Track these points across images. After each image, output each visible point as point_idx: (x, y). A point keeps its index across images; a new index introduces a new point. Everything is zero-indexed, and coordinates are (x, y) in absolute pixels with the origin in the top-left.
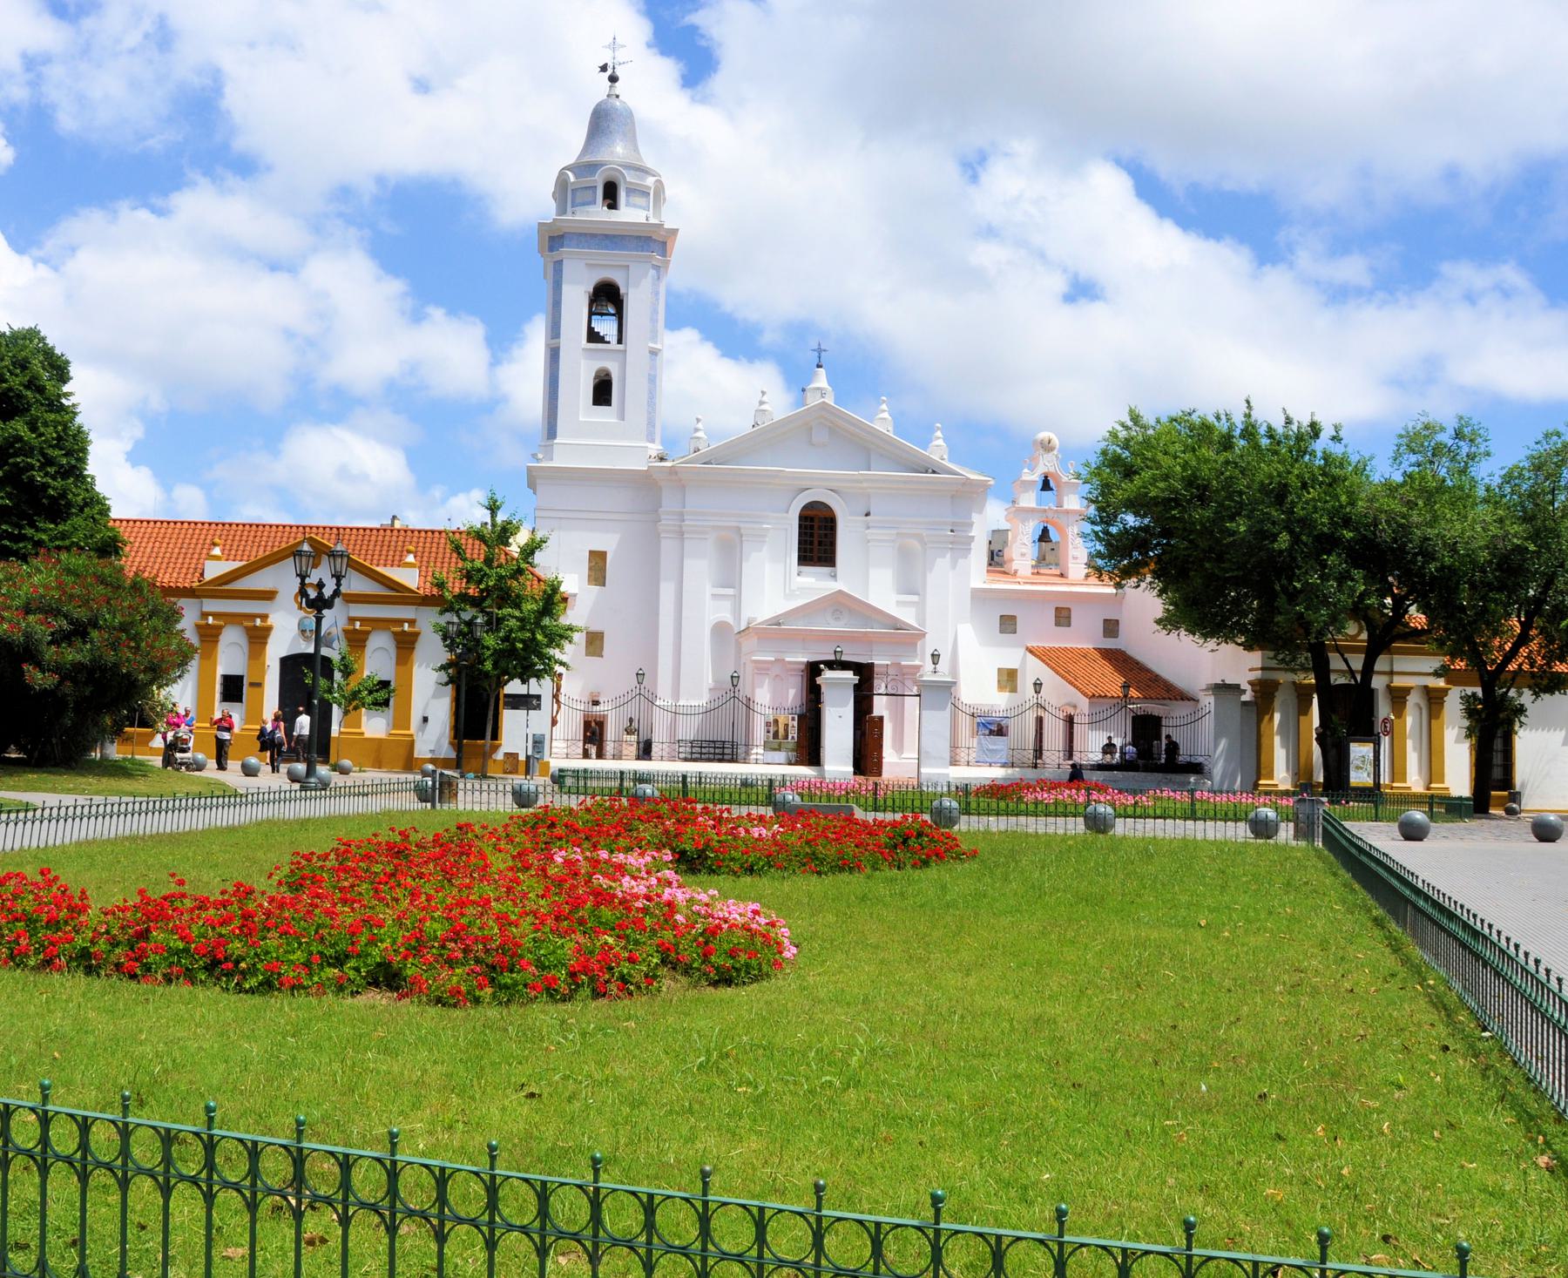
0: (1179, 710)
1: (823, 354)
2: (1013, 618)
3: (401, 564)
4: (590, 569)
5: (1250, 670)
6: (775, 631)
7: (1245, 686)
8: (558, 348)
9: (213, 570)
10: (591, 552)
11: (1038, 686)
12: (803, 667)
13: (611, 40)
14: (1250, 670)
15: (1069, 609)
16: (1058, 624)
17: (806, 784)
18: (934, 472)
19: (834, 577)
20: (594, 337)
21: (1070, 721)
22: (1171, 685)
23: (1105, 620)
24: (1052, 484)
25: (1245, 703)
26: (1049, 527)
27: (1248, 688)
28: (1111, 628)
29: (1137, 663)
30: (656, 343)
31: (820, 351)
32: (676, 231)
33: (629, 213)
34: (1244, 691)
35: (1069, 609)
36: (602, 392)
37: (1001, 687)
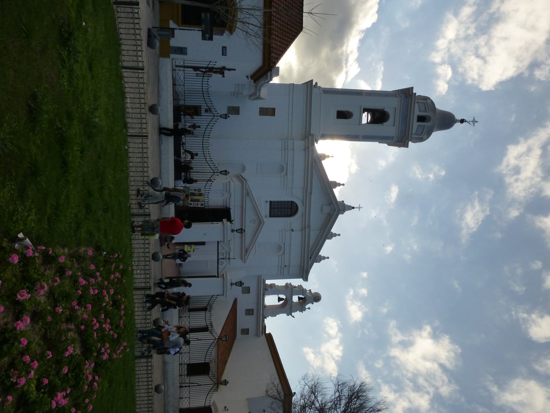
4: (267, 109)
6: (246, 193)
8: (361, 95)
10: (274, 109)
12: (228, 206)
13: (477, 121)
15: (253, 314)
16: (247, 310)
18: (311, 258)
28: (245, 332)
35: (253, 314)
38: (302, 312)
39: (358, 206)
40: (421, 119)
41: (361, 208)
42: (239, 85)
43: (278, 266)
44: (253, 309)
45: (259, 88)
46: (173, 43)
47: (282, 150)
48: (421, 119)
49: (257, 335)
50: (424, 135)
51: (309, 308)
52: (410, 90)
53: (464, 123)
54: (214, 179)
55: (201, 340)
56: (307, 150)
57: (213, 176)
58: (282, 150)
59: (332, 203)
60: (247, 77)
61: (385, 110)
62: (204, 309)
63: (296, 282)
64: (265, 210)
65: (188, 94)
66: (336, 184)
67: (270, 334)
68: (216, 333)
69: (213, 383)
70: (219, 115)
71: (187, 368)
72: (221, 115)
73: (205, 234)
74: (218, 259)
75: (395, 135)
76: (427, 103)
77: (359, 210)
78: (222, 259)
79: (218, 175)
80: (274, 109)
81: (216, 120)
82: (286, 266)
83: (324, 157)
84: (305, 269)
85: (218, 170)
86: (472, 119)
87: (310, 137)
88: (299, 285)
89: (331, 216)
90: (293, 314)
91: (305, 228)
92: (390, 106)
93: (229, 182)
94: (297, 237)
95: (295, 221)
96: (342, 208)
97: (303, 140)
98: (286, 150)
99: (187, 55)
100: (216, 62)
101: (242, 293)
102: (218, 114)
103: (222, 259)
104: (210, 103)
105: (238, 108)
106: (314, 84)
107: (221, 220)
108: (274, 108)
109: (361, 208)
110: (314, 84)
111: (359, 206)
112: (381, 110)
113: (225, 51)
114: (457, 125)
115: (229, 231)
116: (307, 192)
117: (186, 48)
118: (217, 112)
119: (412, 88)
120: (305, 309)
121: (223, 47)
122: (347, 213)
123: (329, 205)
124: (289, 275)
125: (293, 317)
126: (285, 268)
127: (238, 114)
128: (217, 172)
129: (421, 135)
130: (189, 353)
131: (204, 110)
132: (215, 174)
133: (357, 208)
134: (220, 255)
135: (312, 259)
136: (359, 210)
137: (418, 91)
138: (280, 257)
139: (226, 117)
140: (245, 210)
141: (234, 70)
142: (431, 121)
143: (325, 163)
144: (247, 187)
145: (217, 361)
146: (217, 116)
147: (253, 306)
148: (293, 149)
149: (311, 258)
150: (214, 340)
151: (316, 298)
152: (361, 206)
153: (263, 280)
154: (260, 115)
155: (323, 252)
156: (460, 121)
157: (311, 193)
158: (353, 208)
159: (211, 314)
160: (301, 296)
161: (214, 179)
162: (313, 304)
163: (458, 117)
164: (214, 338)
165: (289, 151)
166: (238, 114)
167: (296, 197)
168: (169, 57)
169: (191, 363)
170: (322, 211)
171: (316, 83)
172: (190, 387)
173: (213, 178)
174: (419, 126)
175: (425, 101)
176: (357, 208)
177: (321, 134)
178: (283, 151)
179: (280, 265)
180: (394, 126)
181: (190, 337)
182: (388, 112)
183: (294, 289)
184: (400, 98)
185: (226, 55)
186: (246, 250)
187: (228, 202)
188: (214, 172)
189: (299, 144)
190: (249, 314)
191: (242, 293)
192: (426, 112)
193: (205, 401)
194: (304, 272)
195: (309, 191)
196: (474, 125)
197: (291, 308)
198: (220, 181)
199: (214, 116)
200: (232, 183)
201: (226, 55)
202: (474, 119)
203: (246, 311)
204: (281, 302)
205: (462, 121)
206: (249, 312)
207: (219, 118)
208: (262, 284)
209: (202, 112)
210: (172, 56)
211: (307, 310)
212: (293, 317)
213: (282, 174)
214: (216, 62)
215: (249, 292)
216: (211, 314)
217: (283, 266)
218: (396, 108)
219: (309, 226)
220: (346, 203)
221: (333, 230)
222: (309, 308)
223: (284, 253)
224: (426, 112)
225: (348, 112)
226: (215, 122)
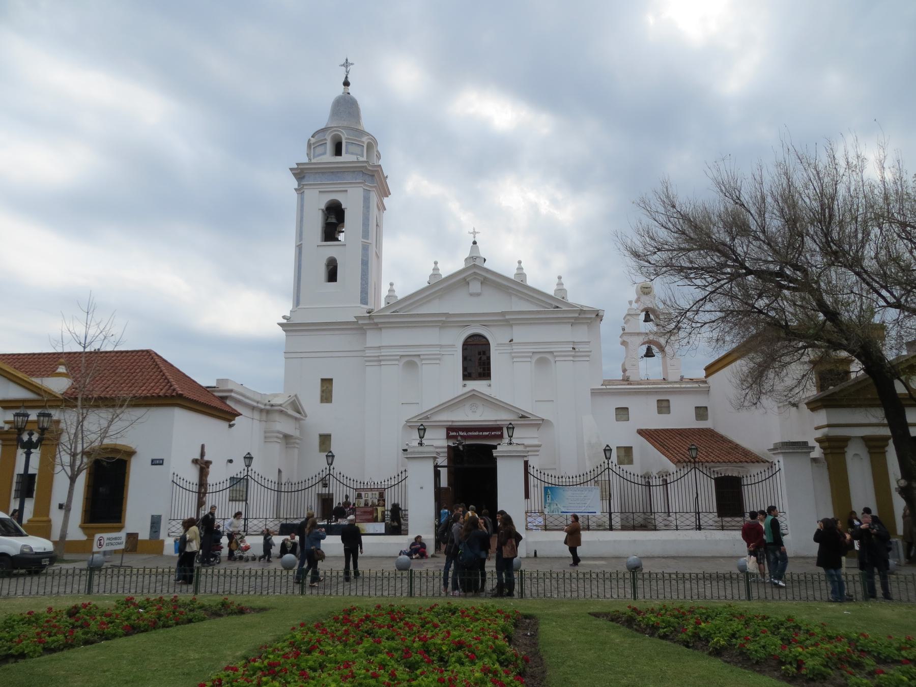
0: (755, 470)
2: (626, 409)
3: (54, 374)
4: (323, 391)
5: (817, 428)
7: (812, 443)
14: (817, 428)
15: (668, 401)
16: (660, 412)
18: (558, 307)
22: (749, 452)
23: (697, 408)
24: (652, 317)
25: (815, 460)
26: (653, 347)
27: (817, 445)
28: (702, 413)
29: (722, 437)
30: (368, 239)
31: (474, 233)
34: (813, 448)
35: (668, 401)
39: (472, 235)
40: (338, 151)
41: (474, 229)
42: (265, 437)
44: (658, 401)
45: (268, 407)
46: (144, 534)
47: (381, 365)
48: (338, 151)
49: (707, 391)
50: (363, 142)
52: (293, 172)
53: (349, 80)
54: (340, 474)
55: (610, 494)
56: (380, 326)
57: (335, 476)
58: (381, 365)
59: (464, 279)
60: (231, 426)
61: (323, 206)
63: (609, 328)
65: (295, 513)
67: (706, 369)
68: (597, 468)
69: (693, 471)
70: (246, 468)
71: (730, 516)
73: (422, 488)
75: (362, 189)
76: (314, 144)
77: (478, 233)
79: (334, 469)
80: (323, 380)
81: (253, 472)
82: (574, 348)
84: (577, 315)
85: (326, 469)
86: (344, 69)
87: (360, 322)
89: (485, 278)
91: (507, 321)
92: (318, 202)
94: (522, 334)
95: (496, 339)
97: (365, 334)
98: (381, 358)
99: (160, 516)
100: (174, 474)
101: (628, 420)
104: (310, 481)
105: (321, 436)
106: (285, 321)
107: (494, 461)
108: (320, 381)
109: (474, 229)
110: (285, 321)
112: (325, 215)
113: (158, 461)
115: (421, 449)
116: (444, 322)
117: (152, 516)
118: (242, 472)
119: (291, 169)
121: (152, 464)
123: (468, 283)
124: (589, 342)
126: (577, 350)
128: (330, 470)
130: (633, 513)
131: (324, 488)
132: (331, 472)
133: (474, 237)
136: (478, 233)
139: (331, 457)
140: (453, 421)
141: (203, 447)
142: (341, 135)
144: (415, 420)
145: (713, 464)
146: (248, 471)
147: (652, 403)
148: (379, 347)
149: (558, 307)
150: (610, 470)
152: (472, 231)
153: (602, 385)
154: (331, 402)
156: (346, 87)
157: (447, 315)
158: (475, 243)
159: (562, 477)
161: (340, 474)
163: (340, 90)
164: (607, 471)
165: (382, 354)
167: (457, 339)
168: (163, 541)
169: (715, 510)
170: (478, 295)
171: (284, 317)
172: (700, 511)
173: (338, 475)
175: (312, 147)
176: (474, 237)
177: (360, 305)
179: (572, 359)
180: (346, 191)
181: (667, 511)
182: (327, 203)
183: (627, 331)
184: (305, 187)
185: (163, 460)
186: (521, 418)
188: (329, 474)
189: (373, 339)
190: (669, 407)
191: (628, 420)
192: (326, 143)
193: (638, 484)
194: (583, 316)
195: (444, 319)
196: (352, 64)
201: (163, 460)
202: (343, 65)
203: (662, 413)
204: (655, 349)
205: (346, 84)
206: (663, 407)
207: (250, 469)
208: (608, 387)
209: (324, 492)
210: (161, 538)
213: (419, 364)
214: (174, 474)
215: (627, 408)
216: (562, 477)
217: (573, 353)
218: (320, 192)
219: (503, 314)
220: (467, 255)
221: (511, 273)
223: (552, 352)
224: (326, 143)
226: (256, 474)
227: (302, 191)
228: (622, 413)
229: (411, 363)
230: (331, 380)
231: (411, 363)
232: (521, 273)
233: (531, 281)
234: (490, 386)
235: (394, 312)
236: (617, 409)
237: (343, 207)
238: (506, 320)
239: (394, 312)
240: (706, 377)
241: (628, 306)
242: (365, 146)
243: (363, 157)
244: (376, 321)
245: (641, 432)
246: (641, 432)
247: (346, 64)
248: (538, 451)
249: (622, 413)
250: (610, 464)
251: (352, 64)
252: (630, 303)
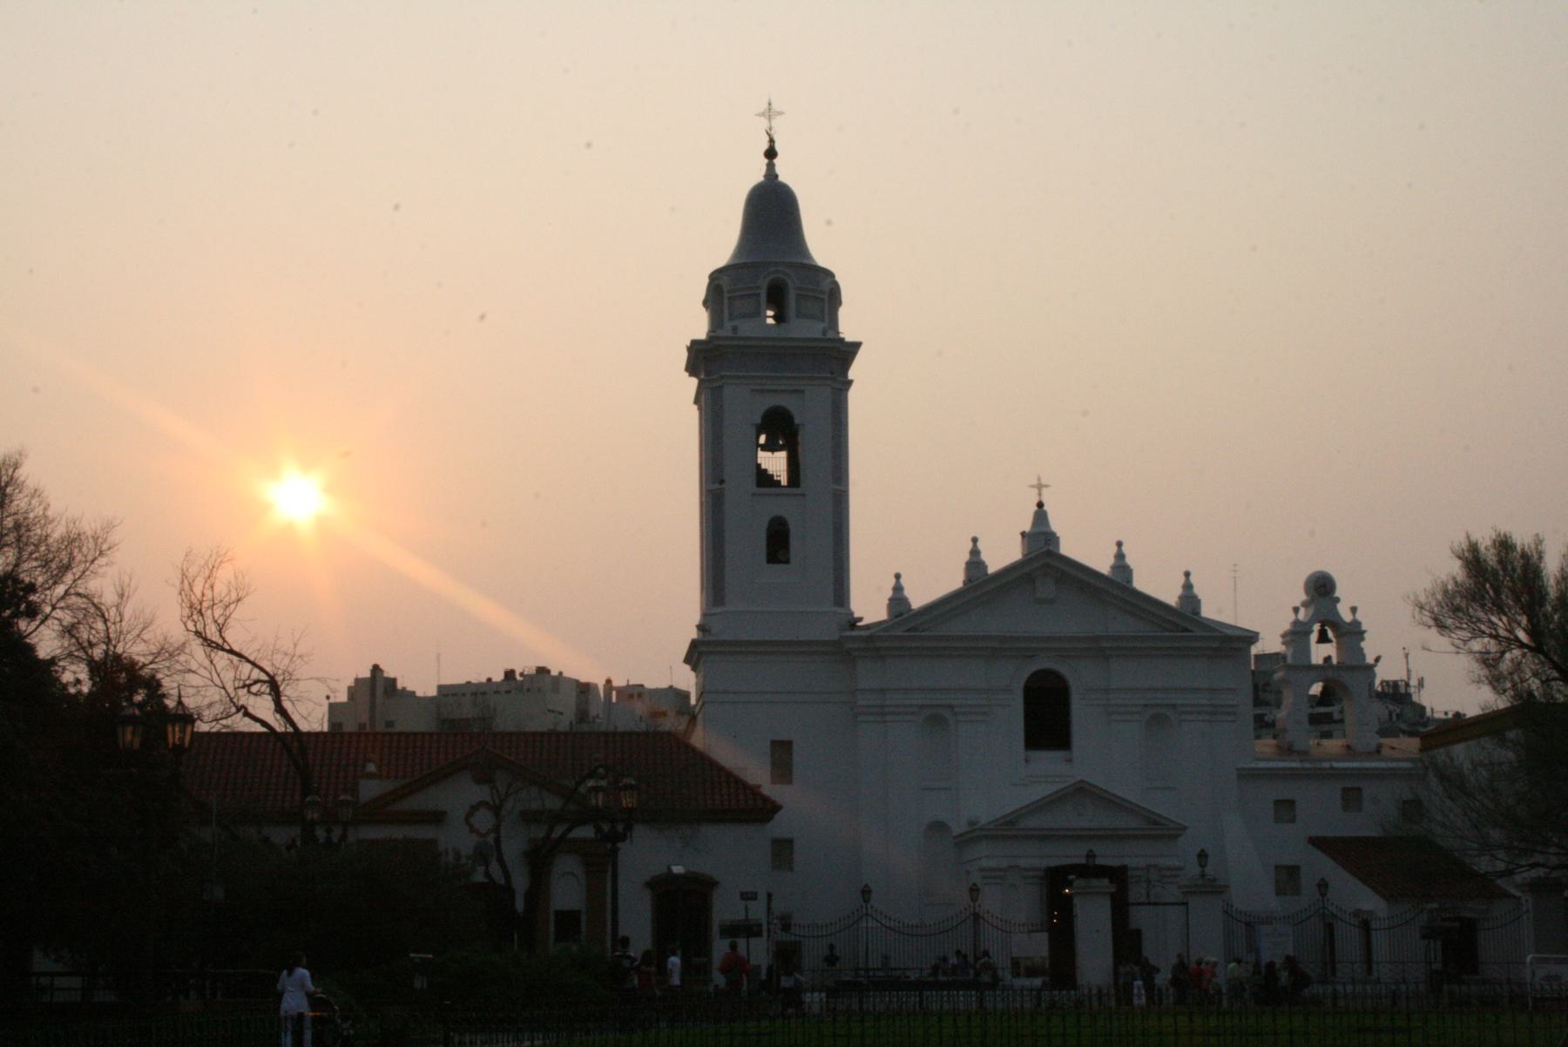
1: (1044, 491)
2: (1291, 803)
6: (1007, 829)
9: (370, 789)
11: (1323, 886)
13: (766, 106)
15: (1359, 789)
16: (1346, 807)
17: (1094, 992)
18: (1187, 630)
19: (1070, 761)
20: (764, 478)
21: (1366, 926)
24: (1330, 634)
32: (857, 345)
33: (803, 329)
35: (1359, 789)
36: (778, 542)
37: (1279, 892)
38: (1364, 632)
39: (1035, 491)
41: (1039, 479)
43: (1210, 721)
47: (886, 722)
51: (1354, 610)
58: (886, 722)
62: (1330, 928)
64: (1048, 761)
66: (975, 563)
70: (864, 905)
72: (865, 901)
74: (1149, 904)
77: (1046, 486)
78: (1148, 895)
80: (773, 743)
83: (898, 600)
84: (1216, 644)
88: (1280, 640)
90: (1370, 660)
92: (747, 405)
93: (982, 870)
95: (1081, 678)
96: (1040, 538)
98: (886, 710)
102: (862, 907)
103: (1148, 895)
109: (1039, 479)
111: (1033, 486)
114: (785, 175)
120: (1356, 624)
122: (1055, 525)
125: (1378, 659)
127: (790, 842)
129: (823, 300)
133: (1040, 494)
134: (1140, 901)
135: (1190, 628)
137: (700, 326)
138: (1183, 717)
142: (781, 276)
143: (918, 598)
148: (883, 691)
149: (1187, 630)
151: (1321, 588)
152: (1035, 482)
155: (1170, 595)
158: (1040, 505)
160: (1314, 637)
162: (1338, 600)
165: (888, 702)
166: (790, 842)
167: (1013, 678)
174: (800, 315)
176: (1040, 494)
178: (888, 718)
179: (1207, 717)
187: (1031, 873)
196: (781, 113)
197: (1352, 668)
198: (991, 902)
199: (867, 914)
200: (985, 863)
202: (762, 114)
206: (1351, 798)
211: (1359, 617)
212: (1378, 659)
218: (753, 390)
220: (1027, 526)
221: (1102, 564)
222: (1354, 610)
223: (1174, 706)
225: (768, 529)
227: (720, 383)
228: (1285, 809)
229: (936, 720)
230: (790, 743)
231: (936, 720)
232: (1122, 567)
233: (1141, 583)
234: (1070, 761)
235: (908, 631)
236: (1277, 803)
237: (797, 421)
238: (1099, 650)
239: (908, 631)
240: (1421, 750)
241: (1292, 617)
242: (826, 297)
243: (823, 320)
244: (879, 644)
245: (1318, 843)
246: (1318, 843)
247: (769, 113)
248: (1176, 876)
249: (1285, 809)
250: (1326, 902)
251: (781, 113)
252: (1296, 610)
